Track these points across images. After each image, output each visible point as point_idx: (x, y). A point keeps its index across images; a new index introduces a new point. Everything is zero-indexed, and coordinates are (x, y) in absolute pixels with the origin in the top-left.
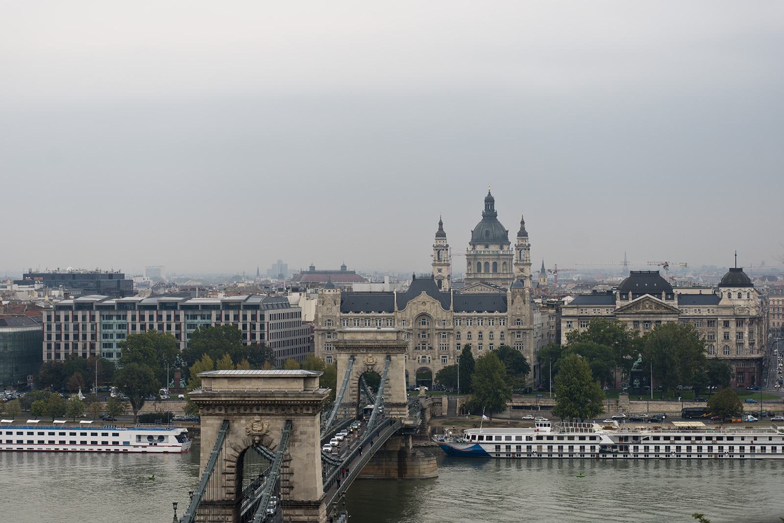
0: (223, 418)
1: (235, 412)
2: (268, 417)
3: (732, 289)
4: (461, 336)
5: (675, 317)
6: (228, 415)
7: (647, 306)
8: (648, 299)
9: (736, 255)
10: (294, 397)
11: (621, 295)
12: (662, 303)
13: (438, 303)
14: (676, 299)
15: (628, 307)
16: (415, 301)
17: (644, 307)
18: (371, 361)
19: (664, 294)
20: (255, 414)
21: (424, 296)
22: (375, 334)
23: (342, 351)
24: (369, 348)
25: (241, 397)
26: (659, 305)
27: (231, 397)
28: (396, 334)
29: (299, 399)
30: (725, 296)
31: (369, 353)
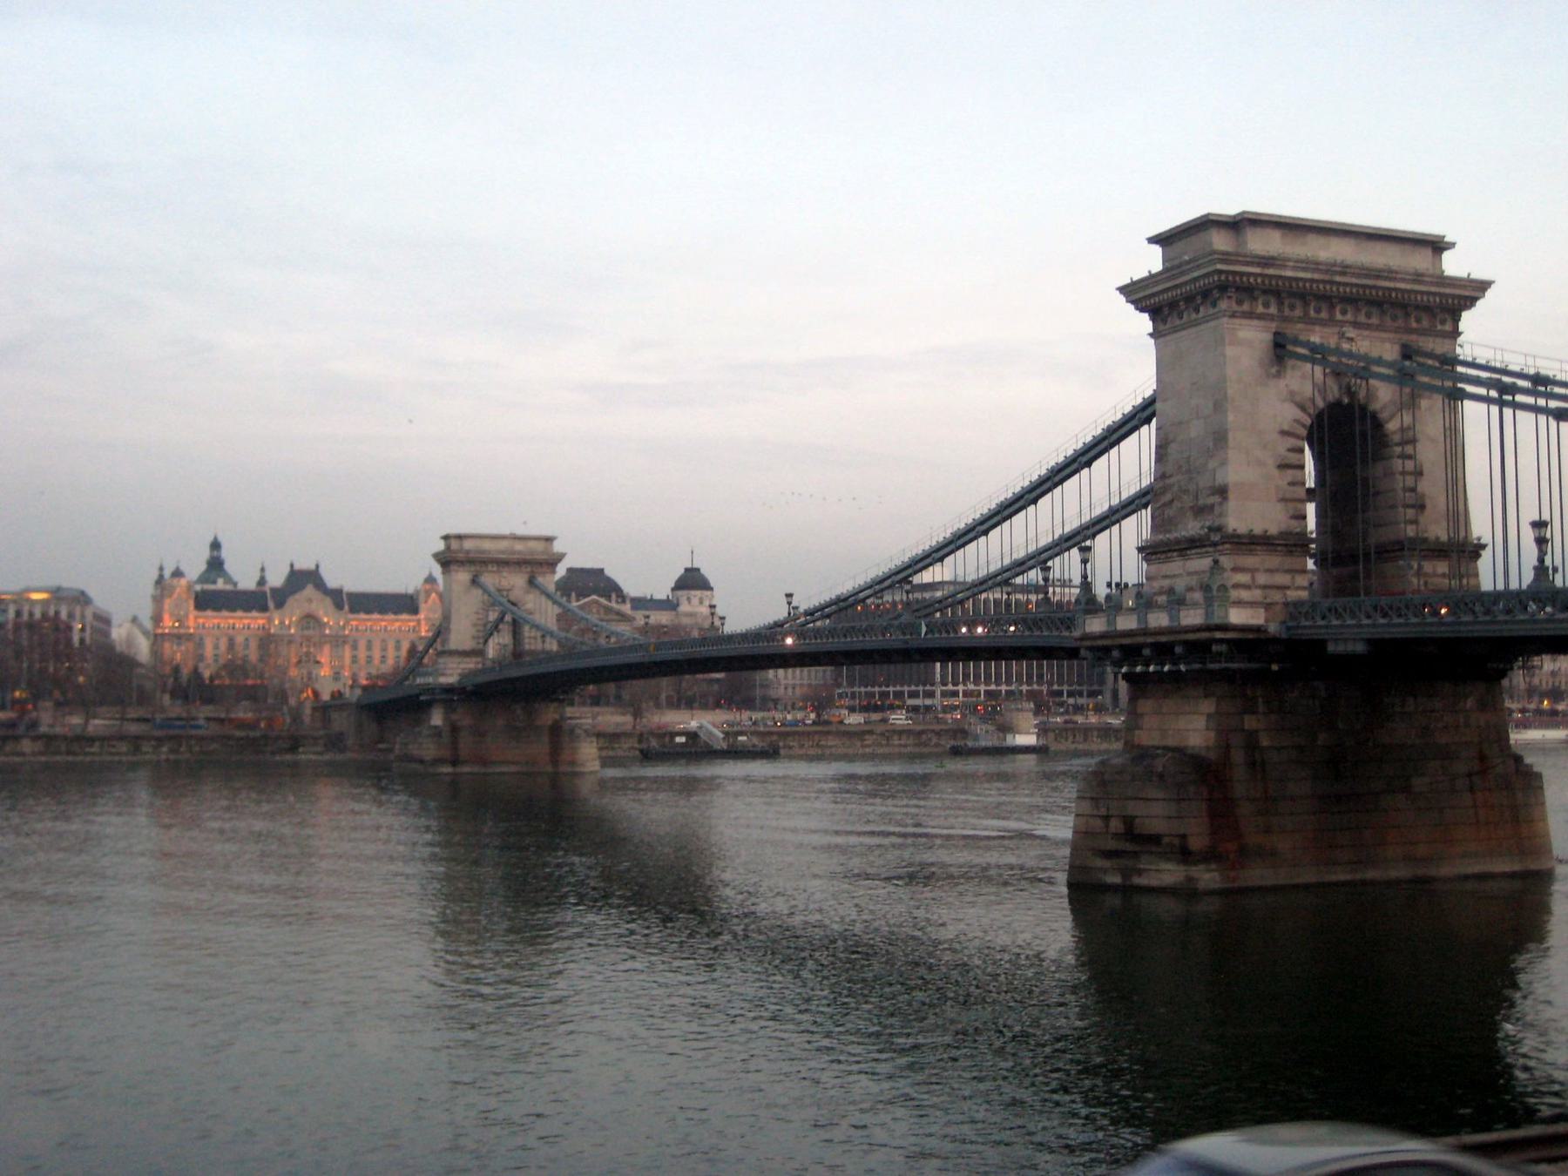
0: (1274, 326)
1: (1298, 312)
2: (1366, 333)
3: (693, 592)
6: (1285, 319)
8: (596, 602)
10: (1432, 284)
13: (328, 601)
16: (297, 596)
19: (614, 596)
20: (1342, 323)
21: (309, 591)
24: (503, 563)
25: (1327, 272)
26: (608, 610)
27: (1304, 269)
29: (1442, 290)
30: (684, 601)
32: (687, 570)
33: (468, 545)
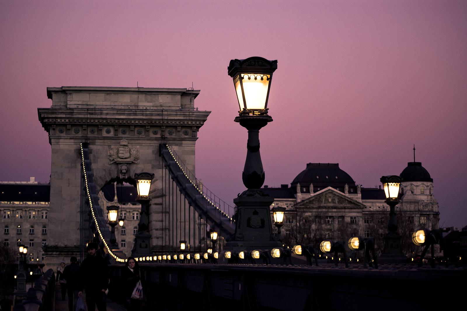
3: (415, 183)
4: (126, 232)
5: (358, 212)
7: (330, 200)
9: (414, 149)
11: (302, 187)
12: (345, 196)
14: (359, 192)
15: (310, 201)
17: (327, 200)
18: (127, 155)
19: (347, 187)
22: (135, 96)
23: (61, 132)
26: (342, 199)
28: (179, 97)
31: (121, 138)
32: (410, 164)
33: (74, 101)
